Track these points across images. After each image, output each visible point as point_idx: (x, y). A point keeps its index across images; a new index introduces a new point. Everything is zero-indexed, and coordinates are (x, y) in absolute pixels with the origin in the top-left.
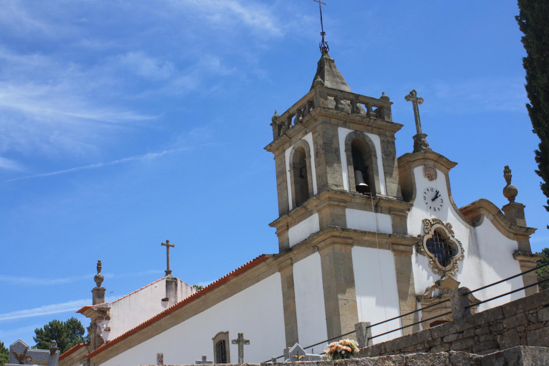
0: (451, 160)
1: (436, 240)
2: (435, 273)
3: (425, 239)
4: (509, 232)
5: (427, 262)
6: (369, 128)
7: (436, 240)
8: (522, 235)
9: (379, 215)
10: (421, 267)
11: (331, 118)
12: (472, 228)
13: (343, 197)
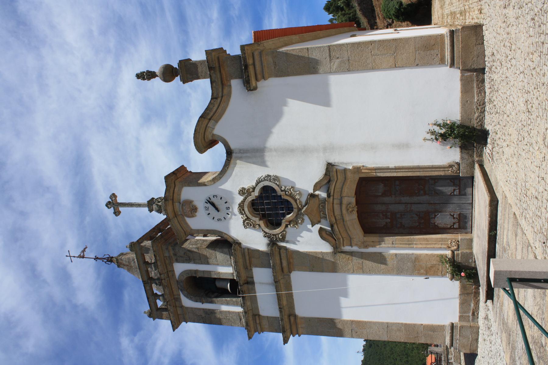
0: (165, 188)
1: (263, 210)
2: (303, 220)
3: (267, 230)
4: (222, 97)
5: (292, 229)
6: (170, 274)
7: (263, 210)
8: (220, 71)
9: (256, 279)
10: (299, 238)
11: (178, 315)
12: (234, 155)
13: (251, 319)
